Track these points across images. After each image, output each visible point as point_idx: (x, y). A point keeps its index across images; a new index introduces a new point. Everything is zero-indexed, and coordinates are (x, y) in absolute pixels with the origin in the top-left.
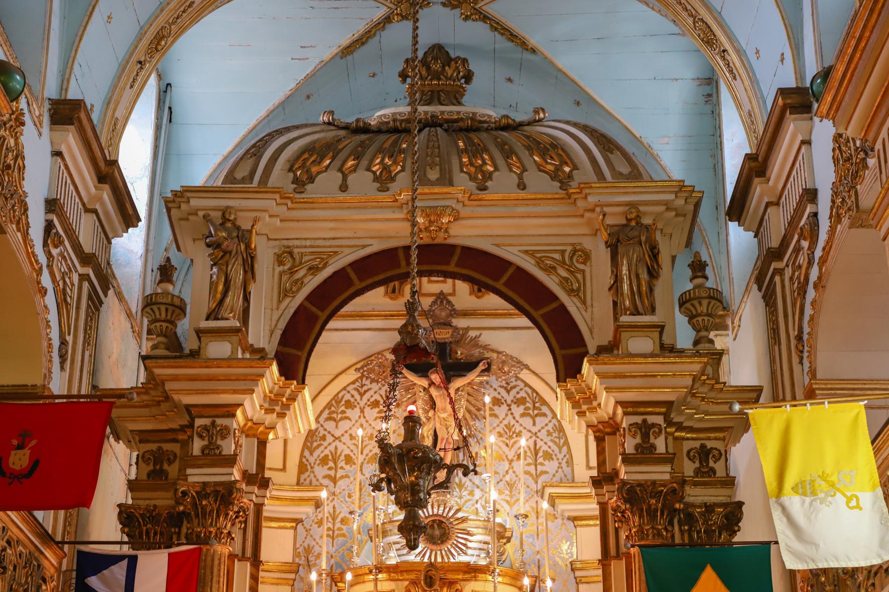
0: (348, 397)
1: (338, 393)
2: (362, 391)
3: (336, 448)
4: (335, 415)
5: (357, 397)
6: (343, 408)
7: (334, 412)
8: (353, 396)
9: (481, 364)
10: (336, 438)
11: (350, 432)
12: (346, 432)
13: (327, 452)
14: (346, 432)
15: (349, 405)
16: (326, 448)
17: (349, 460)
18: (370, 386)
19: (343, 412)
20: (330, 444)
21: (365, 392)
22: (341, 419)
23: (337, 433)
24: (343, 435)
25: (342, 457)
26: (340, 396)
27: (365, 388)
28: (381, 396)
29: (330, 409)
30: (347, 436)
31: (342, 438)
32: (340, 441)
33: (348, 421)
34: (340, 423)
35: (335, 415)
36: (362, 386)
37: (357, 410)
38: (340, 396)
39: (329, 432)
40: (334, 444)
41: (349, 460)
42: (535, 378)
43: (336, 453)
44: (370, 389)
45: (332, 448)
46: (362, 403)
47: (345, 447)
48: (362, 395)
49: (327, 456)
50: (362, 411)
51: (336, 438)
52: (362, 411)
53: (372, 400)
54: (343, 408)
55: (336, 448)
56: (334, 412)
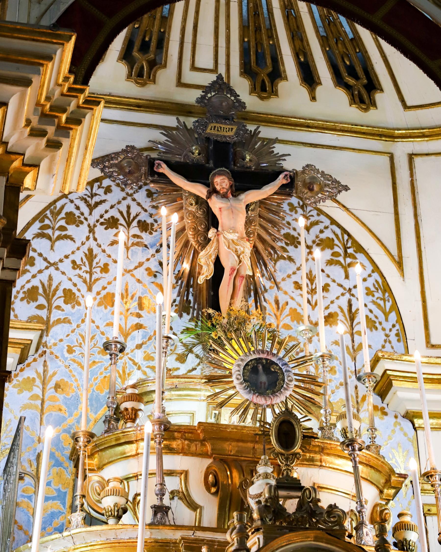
0: (70, 208)
1: (55, 202)
2: (93, 202)
3: (50, 278)
4: (49, 232)
5: (85, 209)
6: (62, 223)
7: (48, 227)
8: (78, 208)
9: (281, 176)
10: (52, 265)
11: (72, 257)
12: (67, 257)
13: (35, 282)
14: (67, 257)
15: (71, 219)
16: (34, 276)
17: (69, 296)
18: (103, 197)
19: (62, 228)
20: (40, 272)
21: (97, 204)
22: (59, 238)
23: (53, 257)
24: (61, 261)
25: (60, 293)
26: (59, 205)
27: (97, 199)
28: (121, 213)
29: (42, 221)
30: (67, 263)
31: (60, 265)
32: (57, 269)
33: (69, 241)
34: (57, 243)
35: (49, 232)
36: (93, 196)
37: (84, 228)
38: (59, 205)
39: (40, 255)
40: (47, 273)
41: (69, 296)
42: (345, 214)
43: (50, 285)
44: (104, 201)
45: (44, 277)
46: (92, 220)
47: (64, 278)
48: (91, 208)
49: (34, 289)
50: (91, 230)
51: (52, 265)
52: (91, 230)
53: (107, 216)
54: (62, 223)
55: (50, 278)
56: (48, 227)
